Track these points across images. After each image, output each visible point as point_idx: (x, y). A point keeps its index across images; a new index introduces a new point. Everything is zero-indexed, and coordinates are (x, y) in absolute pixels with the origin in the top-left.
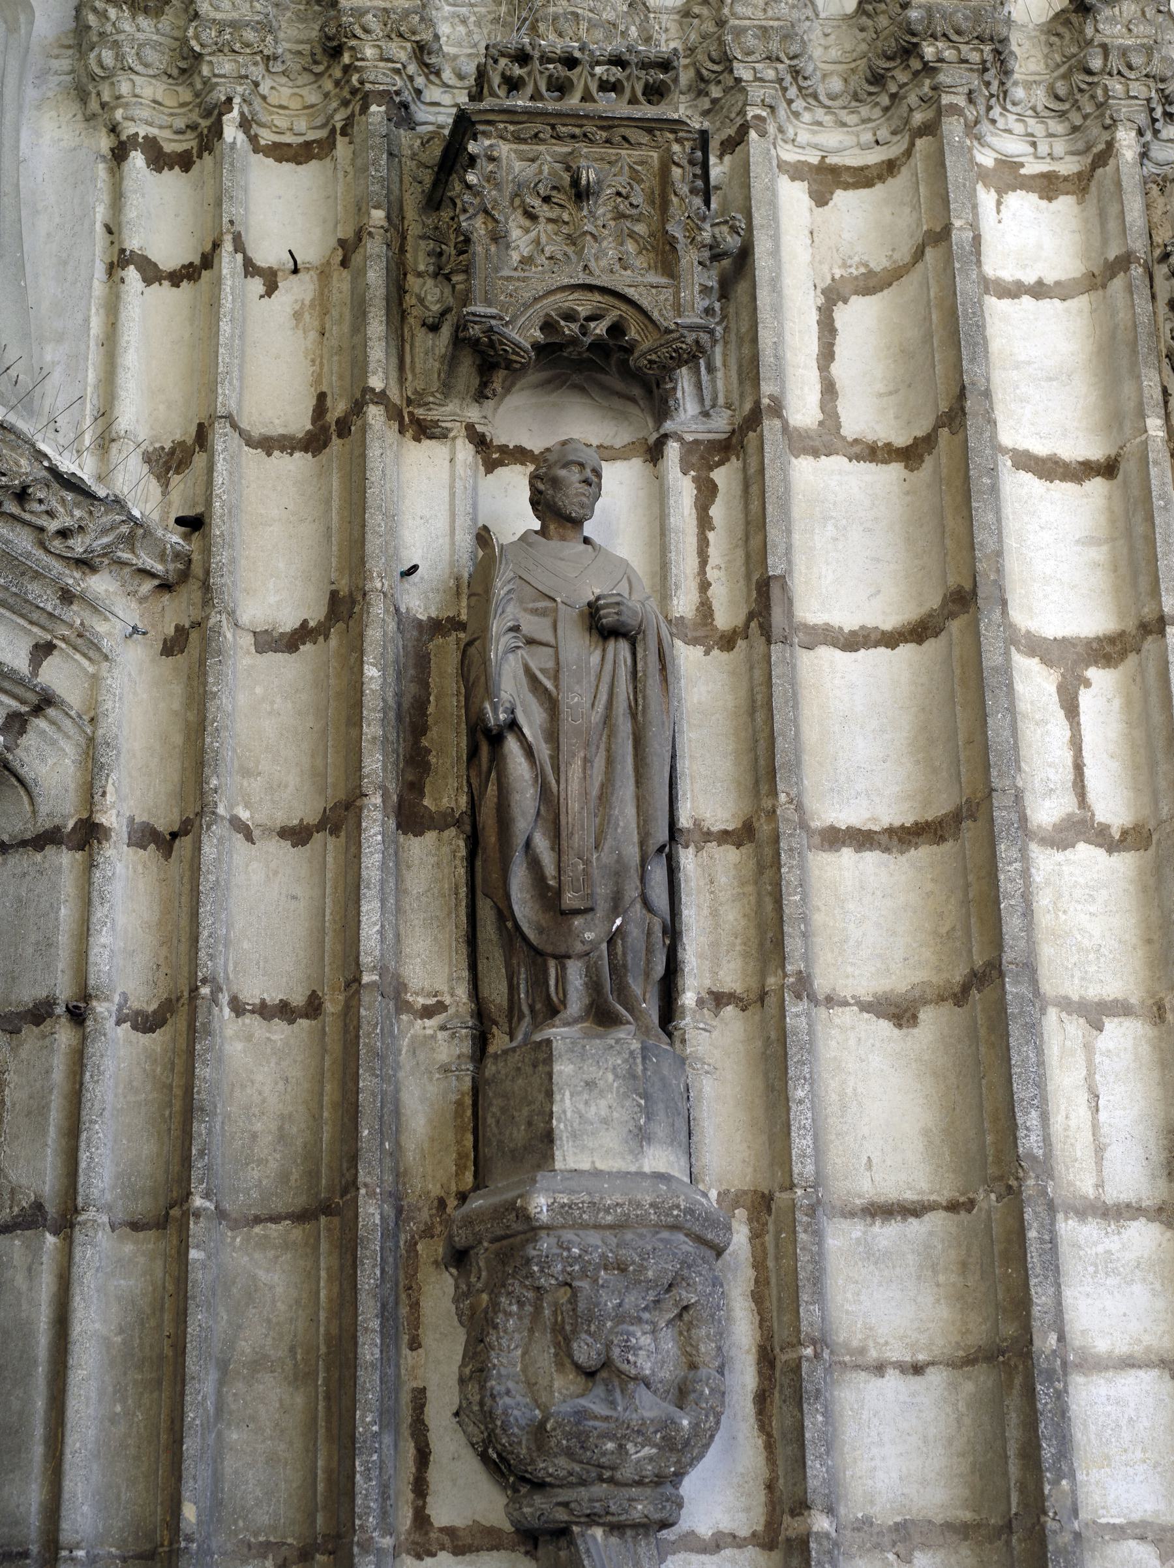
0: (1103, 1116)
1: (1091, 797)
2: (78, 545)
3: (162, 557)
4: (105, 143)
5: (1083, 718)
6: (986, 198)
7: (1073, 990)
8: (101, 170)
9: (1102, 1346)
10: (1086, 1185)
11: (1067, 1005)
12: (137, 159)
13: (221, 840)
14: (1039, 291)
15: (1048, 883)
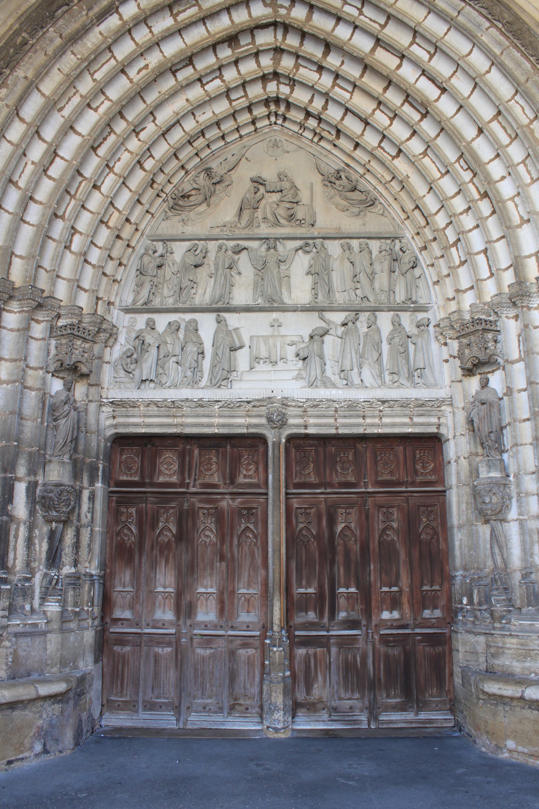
2: (436, 406)
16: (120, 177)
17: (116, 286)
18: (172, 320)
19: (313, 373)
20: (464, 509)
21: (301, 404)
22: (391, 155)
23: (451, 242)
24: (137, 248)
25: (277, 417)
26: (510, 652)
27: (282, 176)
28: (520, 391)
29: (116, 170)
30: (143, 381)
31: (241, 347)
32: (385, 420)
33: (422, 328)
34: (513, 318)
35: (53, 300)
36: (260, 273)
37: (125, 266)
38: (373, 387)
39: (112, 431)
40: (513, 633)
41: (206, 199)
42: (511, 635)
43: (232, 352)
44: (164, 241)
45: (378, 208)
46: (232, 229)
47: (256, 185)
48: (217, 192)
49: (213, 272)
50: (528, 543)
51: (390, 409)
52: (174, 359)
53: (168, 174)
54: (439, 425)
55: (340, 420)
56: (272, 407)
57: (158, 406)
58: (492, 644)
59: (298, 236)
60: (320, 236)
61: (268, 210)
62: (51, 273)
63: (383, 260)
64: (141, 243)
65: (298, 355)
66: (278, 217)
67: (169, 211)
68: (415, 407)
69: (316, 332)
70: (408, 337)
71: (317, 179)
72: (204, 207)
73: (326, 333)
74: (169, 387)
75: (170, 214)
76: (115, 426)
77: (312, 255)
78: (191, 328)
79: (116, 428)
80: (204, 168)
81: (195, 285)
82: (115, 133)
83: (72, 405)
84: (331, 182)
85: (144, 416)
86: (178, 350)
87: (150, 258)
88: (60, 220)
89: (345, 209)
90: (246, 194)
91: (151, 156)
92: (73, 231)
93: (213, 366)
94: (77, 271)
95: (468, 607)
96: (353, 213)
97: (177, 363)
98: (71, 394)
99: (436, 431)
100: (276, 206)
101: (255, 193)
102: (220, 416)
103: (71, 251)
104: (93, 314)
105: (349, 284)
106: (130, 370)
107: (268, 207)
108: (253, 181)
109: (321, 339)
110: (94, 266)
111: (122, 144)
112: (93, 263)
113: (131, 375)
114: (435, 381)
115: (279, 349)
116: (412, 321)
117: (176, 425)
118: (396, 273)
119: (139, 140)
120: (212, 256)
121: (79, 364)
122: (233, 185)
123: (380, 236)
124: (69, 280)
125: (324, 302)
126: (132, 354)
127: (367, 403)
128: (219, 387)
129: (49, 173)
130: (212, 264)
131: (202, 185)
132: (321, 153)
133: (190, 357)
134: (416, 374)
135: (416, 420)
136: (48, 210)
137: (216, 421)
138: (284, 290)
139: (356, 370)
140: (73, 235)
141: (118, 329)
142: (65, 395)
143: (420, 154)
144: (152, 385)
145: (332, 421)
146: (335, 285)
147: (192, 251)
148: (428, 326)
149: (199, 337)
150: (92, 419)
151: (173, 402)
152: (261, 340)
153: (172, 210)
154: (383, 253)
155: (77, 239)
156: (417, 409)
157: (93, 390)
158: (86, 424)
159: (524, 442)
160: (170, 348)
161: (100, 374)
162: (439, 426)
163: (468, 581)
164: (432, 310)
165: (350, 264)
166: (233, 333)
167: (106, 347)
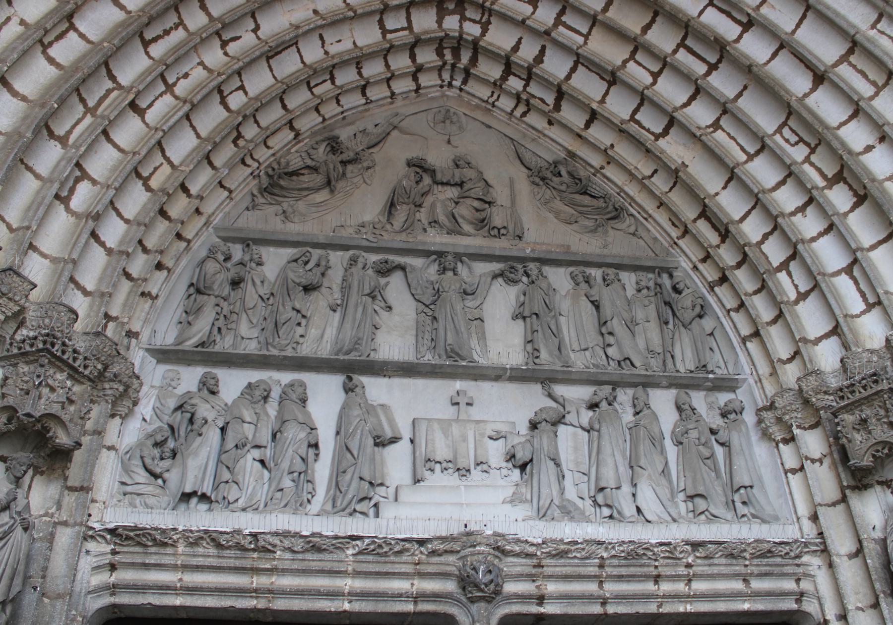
2: (792, 554)
3: (817, 546)
4: (774, 444)
8: (776, 450)
12: (781, 445)
13: (853, 616)
16: (185, 102)
17: (147, 304)
18: (253, 381)
19: (545, 491)
21: (532, 549)
22: (652, 133)
23: (775, 264)
24: (195, 246)
25: (484, 575)
27: (461, 163)
29: (178, 90)
30: (186, 497)
31: (394, 440)
32: (699, 586)
33: (732, 416)
35: (16, 279)
36: (426, 310)
37: (169, 270)
38: (661, 521)
39: (106, 600)
41: (329, 183)
43: (376, 449)
44: (247, 242)
45: (626, 224)
46: (377, 232)
47: (418, 170)
48: (349, 175)
49: (339, 302)
51: (706, 562)
52: (256, 453)
53: (267, 128)
54: (802, 594)
55: (611, 588)
56: (473, 554)
57: (219, 546)
59: (497, 253)
60: (536, 256)
61: (439, 210)
62: (20, 233)
63: (647, 302)
64: (202, 239)
65: (511, 457)
66: (460, 220)
67: (259, 196)
68: (754, 556)
69: (544, 416)
70: (713, 432)
71: (520, 175)
72: (322, 196)
73: (559, 420)
74: (244, 510)
75: (262, 200)
76: (114, 588)
77: (520, 286)
78: (294, 397)
79: (113, 594)
80: (326, 135)
81: (304, 322)
82: (186, 29)
83: (19, 513)
84: (543, 179)
85: (186, 568)
86: (265, 436)
87: (218, 265)
88: (57, 143)
89: (573, 219)
90: (400, 181)
91: (242, 88)
92: (78, 173)
93: (338, 473)
94: (75, 244)
96: (586, 227)
97: (262, 462)
98: (21, 494)
99: (795, 606)
100: (454, 205)
101: (417, 182)
102: (357, 574)
103: (68, 209)
104: (98, 334)
105: (592, 338)
106: (158, 470)
107: (439, 205)
108: (410, 164)
109: (553, 428)
110: (109, 251)
111: (195, 48)
112: (108, 245)
113: (160, 481)
114: (774, 510)
115: (472, 446)
116: (710, 407)
117: (256, 591)
118: (671, 326)
119: (226, 54)
120: (336, 276)
121: (51, 424)
122: (377, 168)
123: (637, 263)
124: (54, 260)
125: (553, 364)
126: (166, 439)
127: (664, 548)
128: (351, 514)
129: (52, 52)
130: (336, 288)
131: (321, 161)
132: (525, 135)
133: (290, 451)
134: (736, 497)
135: (757, 584)
136: (37, 110)
137: (348, 584)
138: (474, 343)
139: (626, 489)
140: (77, 180)
141: (141, 385)
142: (5, 490)
143: (708, 127)
144: (204, 507)
145: (591, 587)
146: (567, 339)
147: (300, 261)
148: (741, 413)
149: (308, 415)
150: (59, 564)
151: (255, 536)
152: (436, 426)
153: (265, 194)
154: (645, 291)
155: (84, 190)
156: (755, 562)
157: (70, 499)
158: (45, 569)
160: (249, 430)
161: (93, 466)
162: (800, 596)
164: (745, 386)
165: (590, 305)
166: (380, 411)
167: (113, 416)
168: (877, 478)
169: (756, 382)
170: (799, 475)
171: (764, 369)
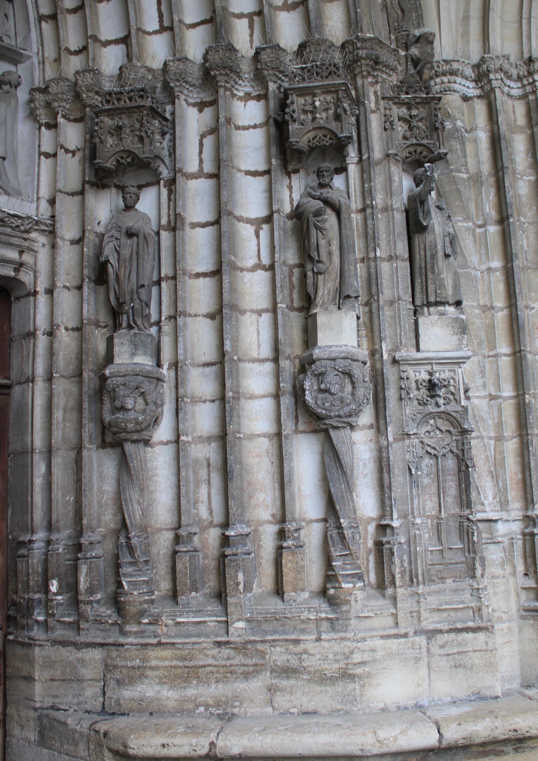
0: (260, 338)
1: (262, 258)
2: (22, 228)
3: (47, 226)
4: (37, 126)
5: (260, 238)
6: (241, 104)
7: (255, 307)
8: (37, 131)
9: (257, 393)
10: (255, 355)
11: (252, 311)
12: (43, 128)
13: (59, 292)
14: (255, 127)
15: (249, 281)
20: (60, 420)
26: (157, 673)
28: (194, 225)
34: (194, 105)
40: (163, 641)
42: (160, 644)
50: (192, 484)
58: (119, 662)
95: (60, 598)
99: (12, 274)
114: (19, 185)
148: (16, 88)
159: (193, 312)
162: (19, 266)
163: (61, 550)
164: (28, 63)
168: (115, 181)
169: (39, 63)
170: (51, 160)
171: (50, 53)
